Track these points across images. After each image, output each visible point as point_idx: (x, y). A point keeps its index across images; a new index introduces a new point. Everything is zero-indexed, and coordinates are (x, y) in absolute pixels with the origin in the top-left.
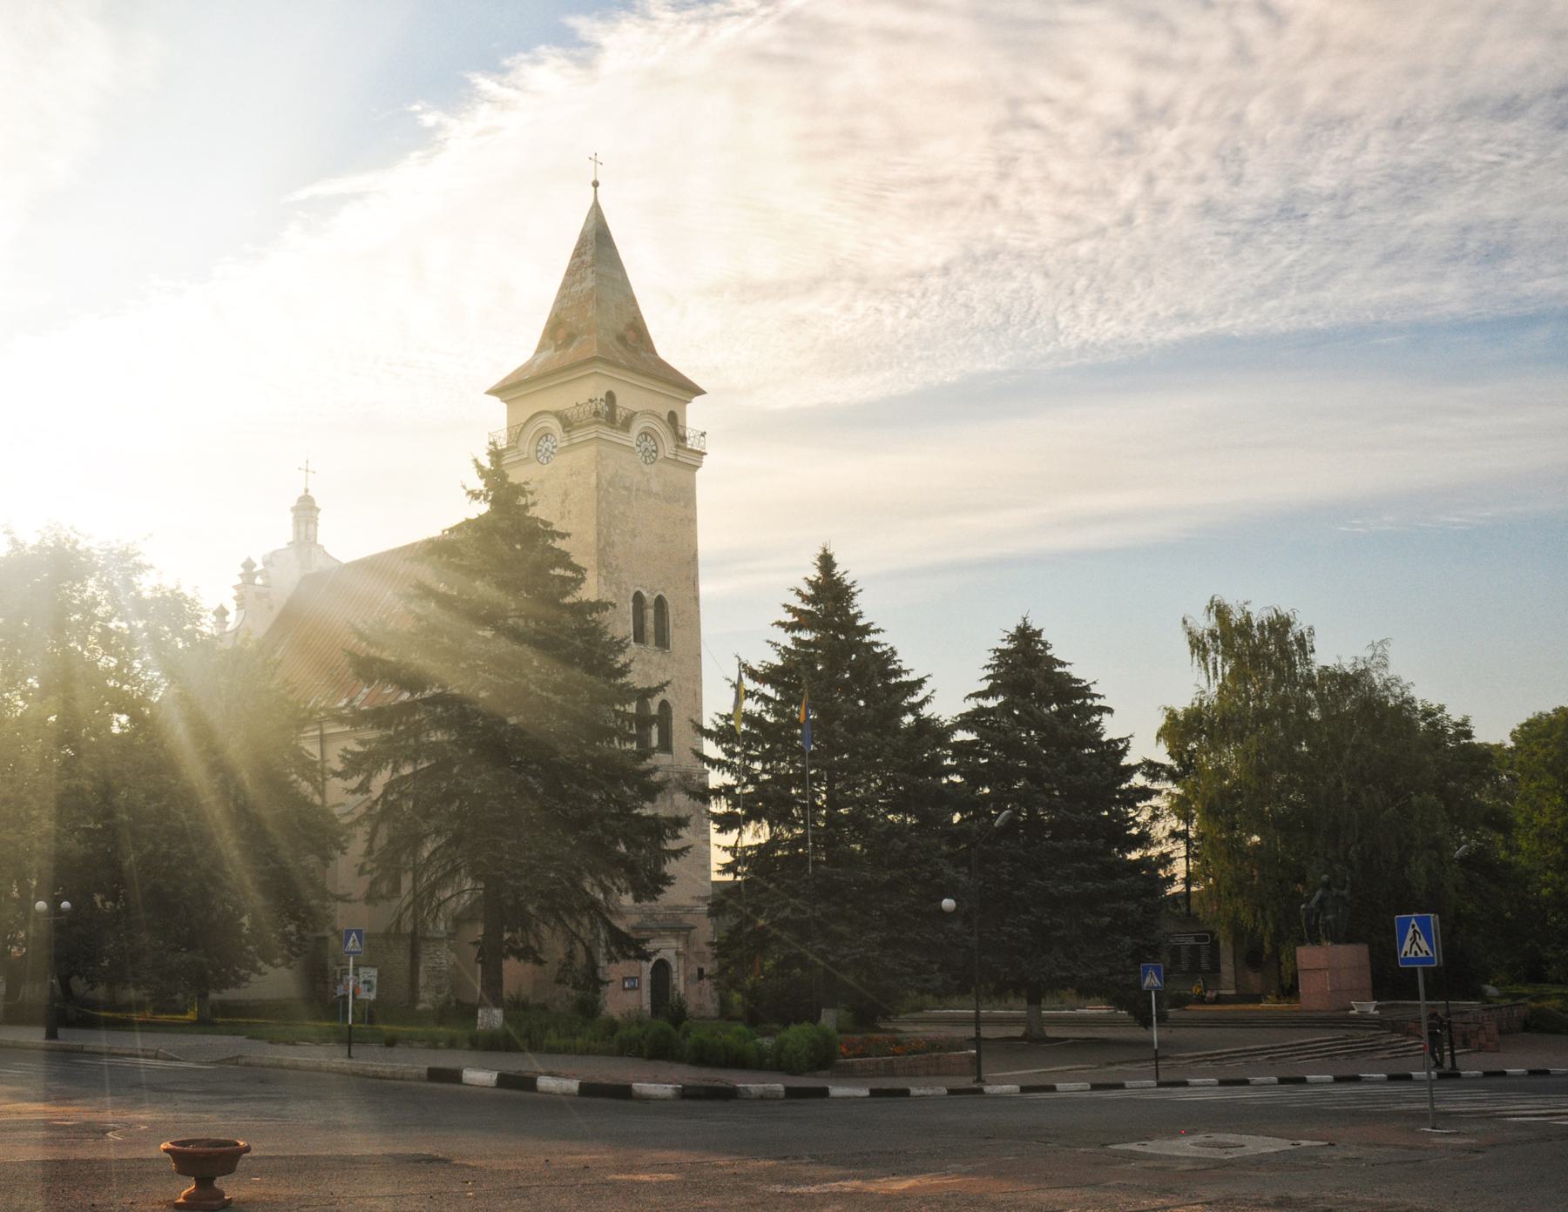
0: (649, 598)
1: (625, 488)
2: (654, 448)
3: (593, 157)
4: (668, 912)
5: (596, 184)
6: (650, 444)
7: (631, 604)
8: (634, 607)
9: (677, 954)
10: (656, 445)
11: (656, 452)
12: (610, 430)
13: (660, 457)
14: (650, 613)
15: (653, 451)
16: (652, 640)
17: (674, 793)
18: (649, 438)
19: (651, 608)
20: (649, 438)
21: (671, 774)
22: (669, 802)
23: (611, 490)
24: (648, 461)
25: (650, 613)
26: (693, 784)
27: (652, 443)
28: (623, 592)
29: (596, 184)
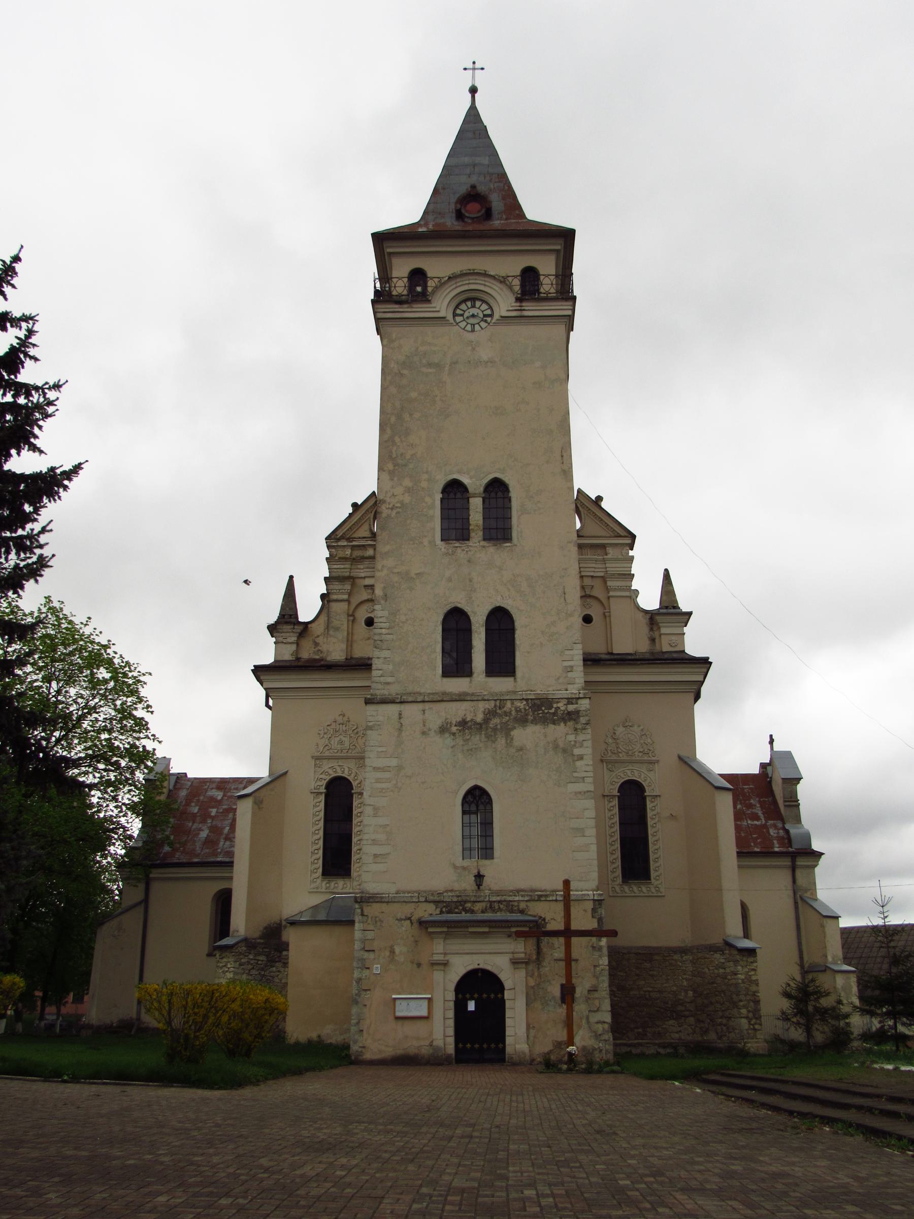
0: (474, 483)
1: (430, 365)
2: (489, 312)
3: (471, 66)
4: (494, 899)
5: (473, 90)
6: (480, 309)
7: (439, 496)
8: (442, 500)
9: (515, 963)
10: (491, 308)
11: (491, 316)
12: (397, 306)
13: (496, 316)
14: (476, 505)
15: (485, 316)
16: (477, 535)
17: (515, 728)
18: (478, 304)
19: (475, 496)
20: (478, 304)
21: (509, 704)
22: (501, 741)
23: (405, 372)
24: (477, 327)
25: (476, 505)
26: (554, 714)
27: (484, 307)
28: (424, 484)
29: (473, 90)
